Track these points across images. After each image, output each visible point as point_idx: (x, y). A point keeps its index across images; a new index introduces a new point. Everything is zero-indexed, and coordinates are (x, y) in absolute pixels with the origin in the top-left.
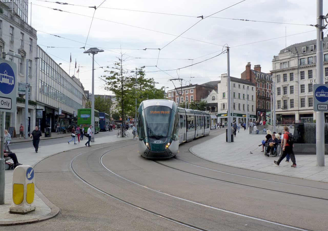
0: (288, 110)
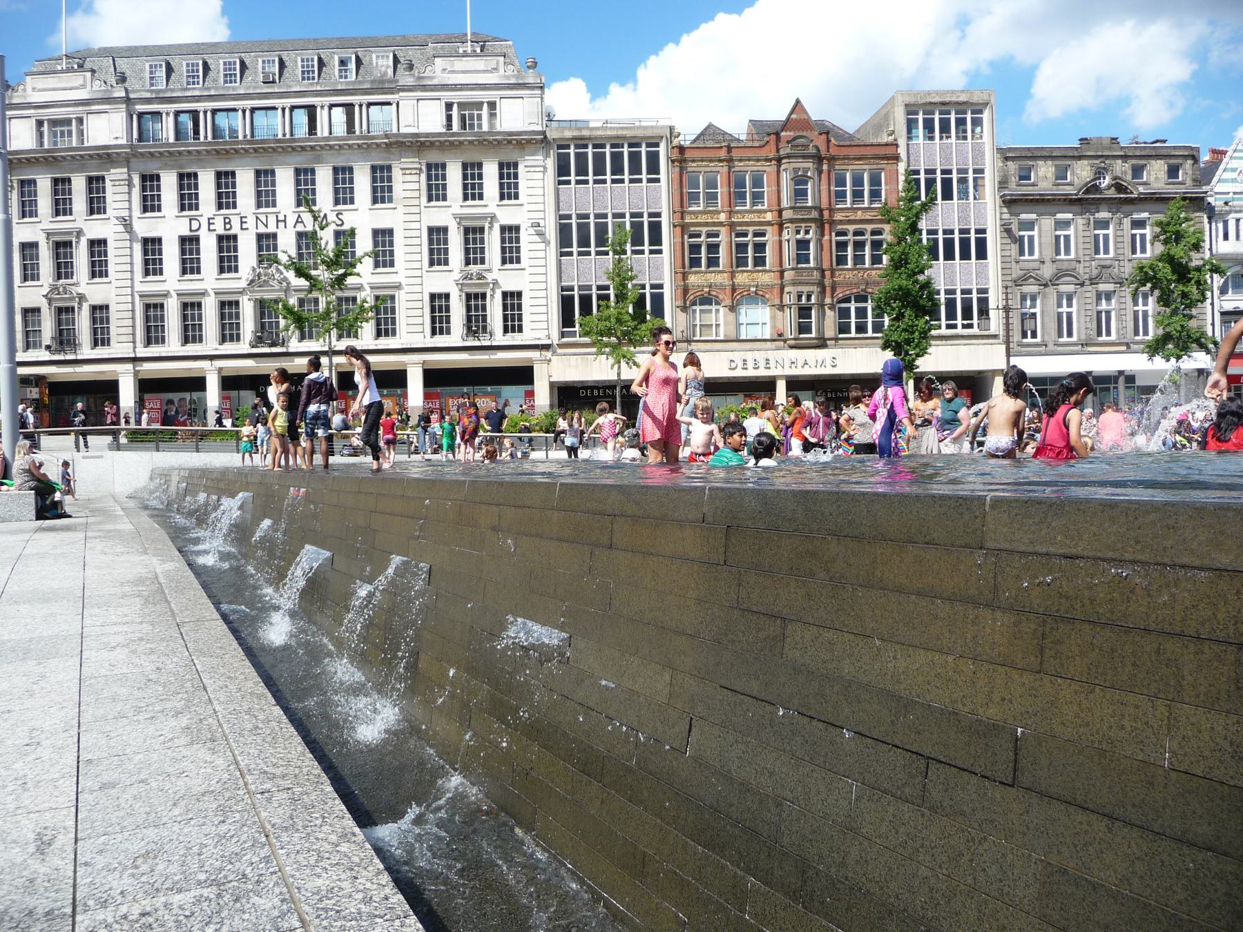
0: (79, 357)
